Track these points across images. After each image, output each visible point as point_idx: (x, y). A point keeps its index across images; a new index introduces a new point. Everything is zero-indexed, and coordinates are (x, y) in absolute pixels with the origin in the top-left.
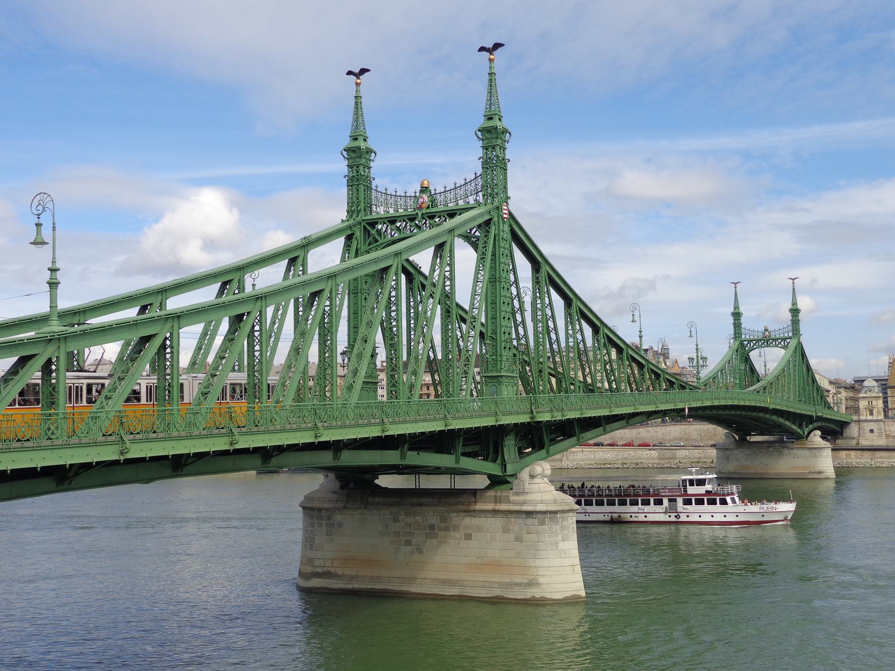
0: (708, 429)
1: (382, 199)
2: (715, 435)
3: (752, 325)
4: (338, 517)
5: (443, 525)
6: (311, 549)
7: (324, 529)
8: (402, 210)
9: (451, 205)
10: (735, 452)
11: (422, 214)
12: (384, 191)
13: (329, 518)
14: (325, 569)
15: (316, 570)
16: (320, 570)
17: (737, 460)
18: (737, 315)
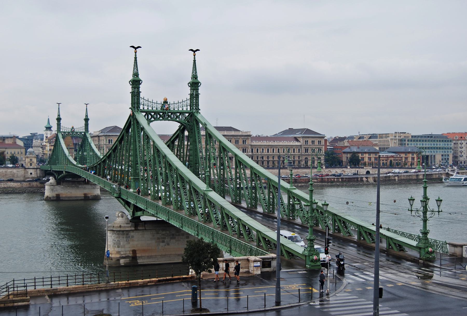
0: (2, 171)
1: (146, 103)
2: (6, 175)
3: (66, 126)
4: (132, 234)
5: (177, 234)
6: (118, 247)
7: (125, 239)
8: (155, 109)
9: (177, 109)
10: (56, 187)
11: (168, 112)
12: (147, 100)
13: (127, 234)
14: (127, 255)
15: (122, 256)
16: (124, 256)
17: (57, 191)
18: (59, 119)
